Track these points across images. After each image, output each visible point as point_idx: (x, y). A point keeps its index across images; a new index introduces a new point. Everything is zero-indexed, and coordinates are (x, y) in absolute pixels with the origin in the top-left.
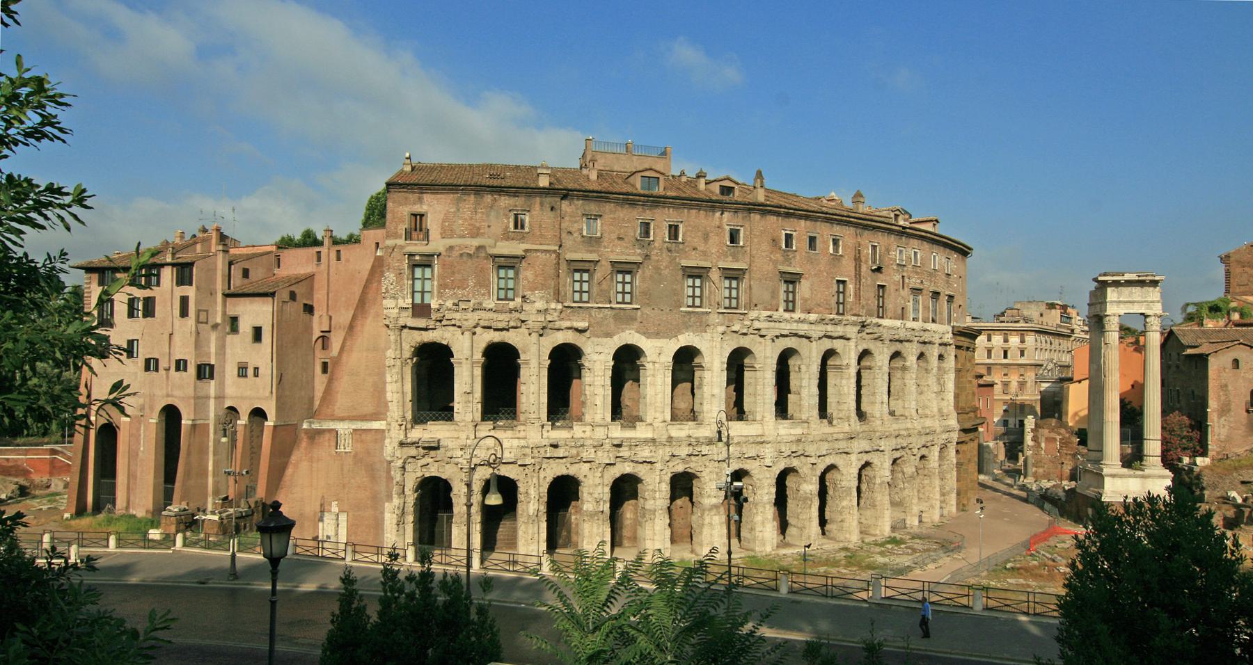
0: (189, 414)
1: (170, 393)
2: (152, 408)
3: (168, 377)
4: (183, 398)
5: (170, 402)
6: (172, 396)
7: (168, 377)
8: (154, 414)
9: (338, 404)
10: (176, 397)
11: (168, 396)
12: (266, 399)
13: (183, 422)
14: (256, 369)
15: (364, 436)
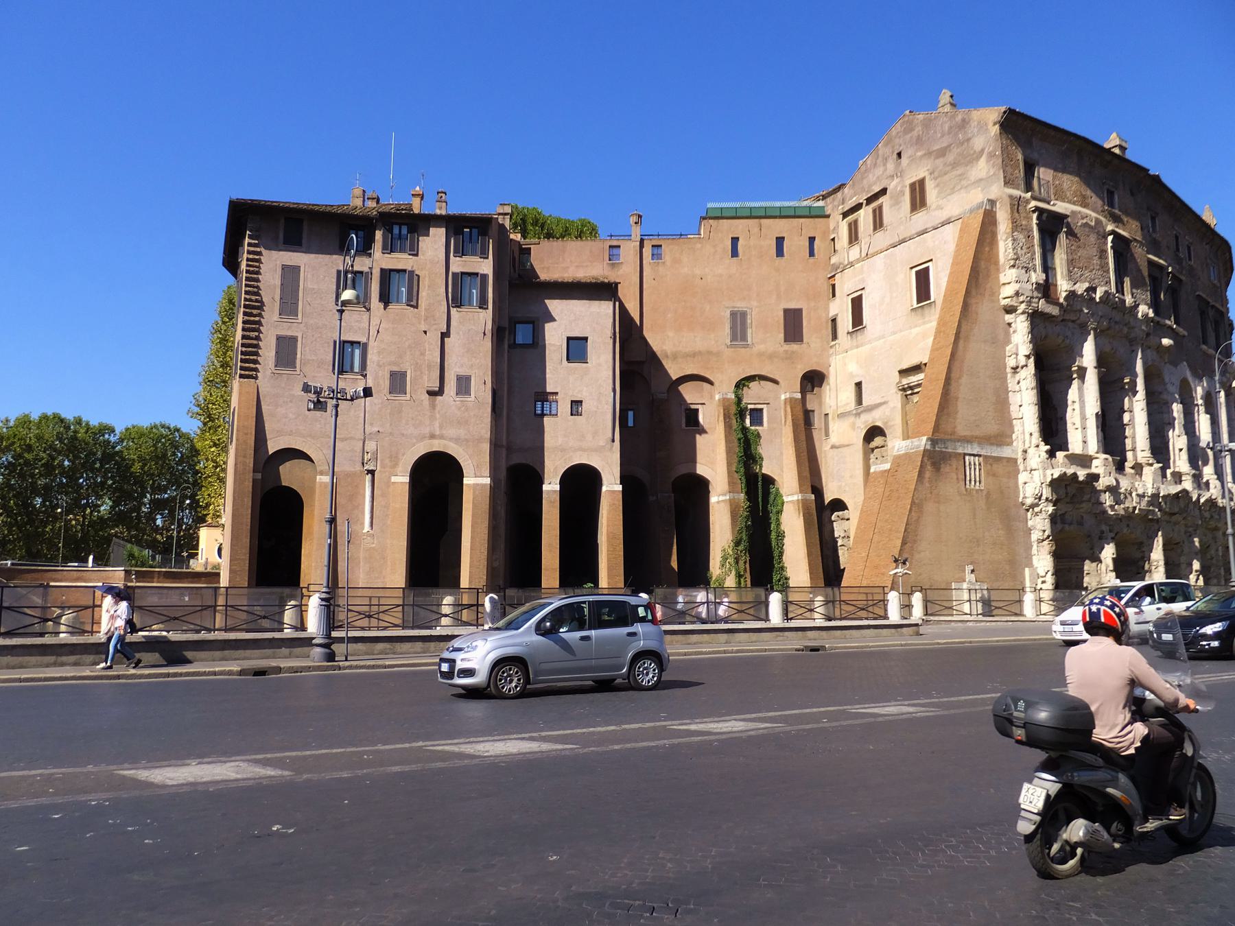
0: (478, 467)
1: (438, 433)
2: (395, 460)
3: (433, 406)
4: (467, 440)
5: (437, 446)
6: (442, 437)
7: (433, 406)
8: (399, 469)
9: (959, 416)
10: (451, 439)
11: (432, 436)
12: (598, 450)
13: (466, 481)
14: (576, 405)
15: (995, 466)
